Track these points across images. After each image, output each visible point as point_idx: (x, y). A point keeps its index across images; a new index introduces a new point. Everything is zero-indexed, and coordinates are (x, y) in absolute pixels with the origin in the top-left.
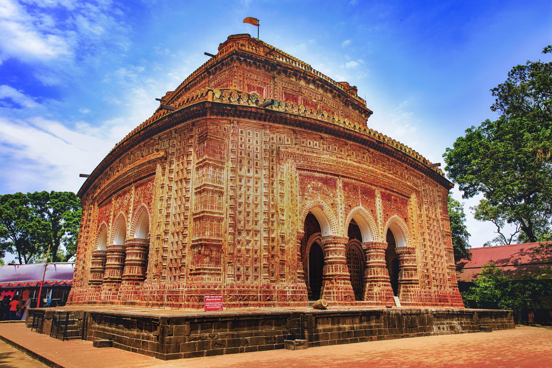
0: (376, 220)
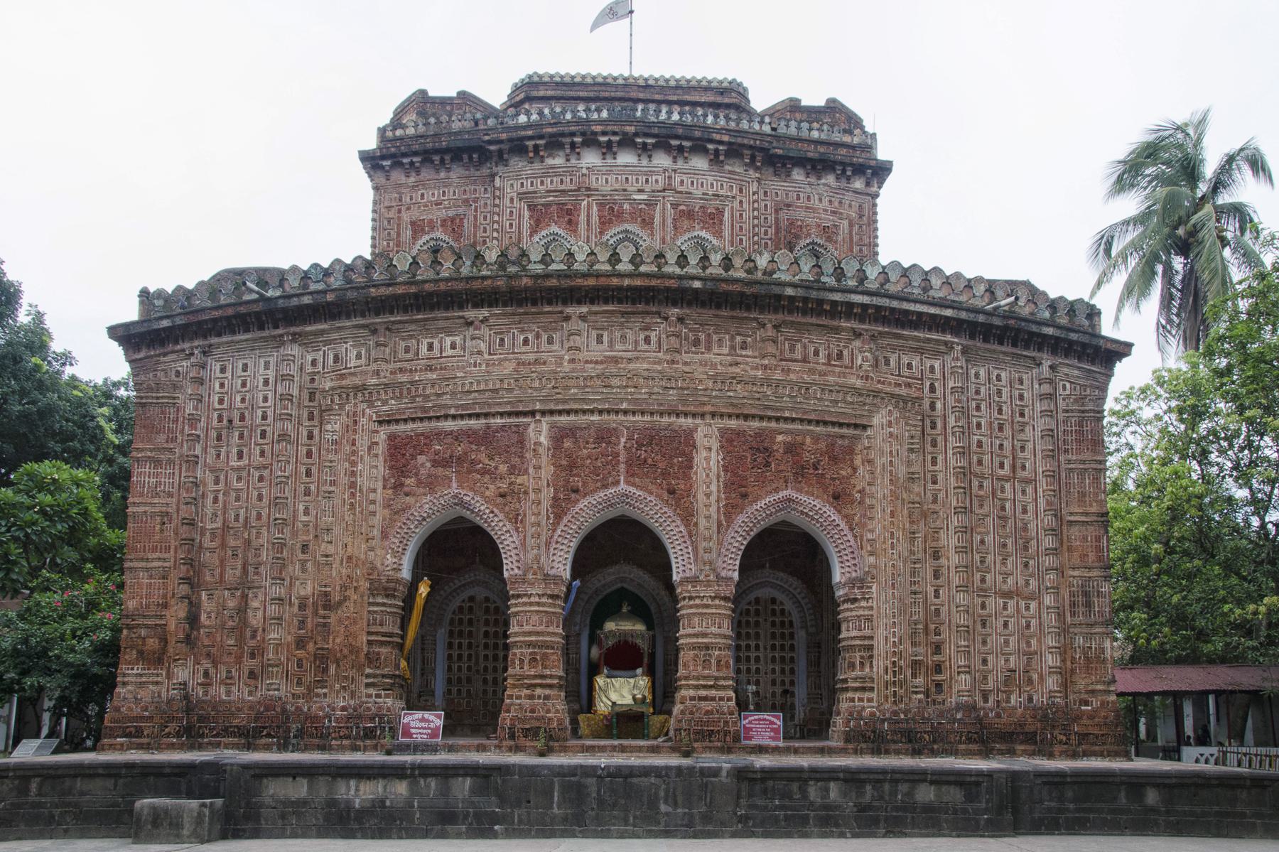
0: (688, 516)
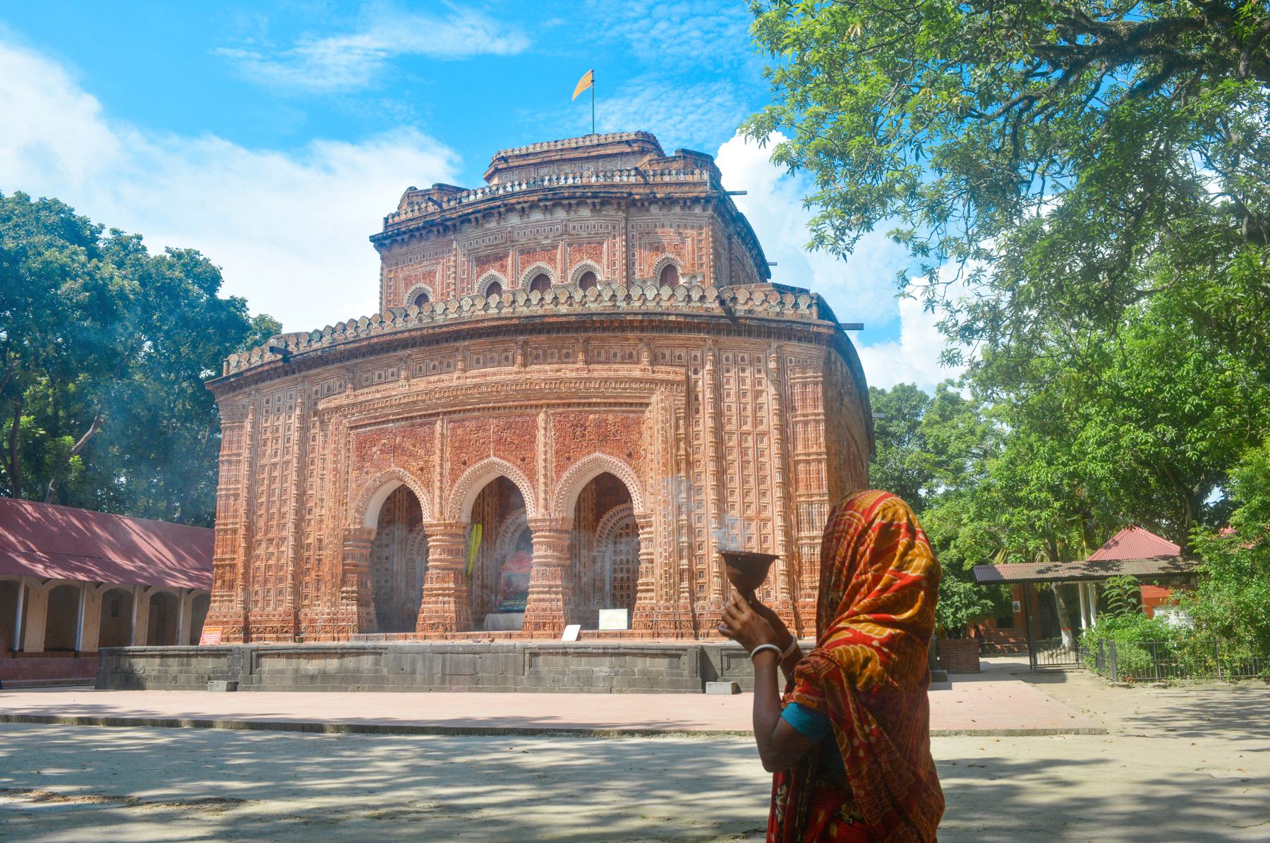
0: (532, 477)
